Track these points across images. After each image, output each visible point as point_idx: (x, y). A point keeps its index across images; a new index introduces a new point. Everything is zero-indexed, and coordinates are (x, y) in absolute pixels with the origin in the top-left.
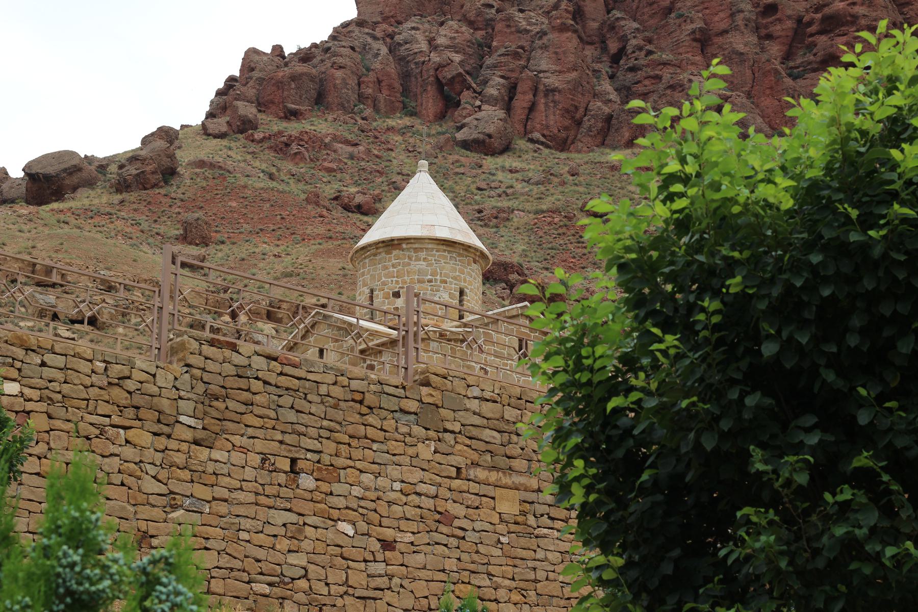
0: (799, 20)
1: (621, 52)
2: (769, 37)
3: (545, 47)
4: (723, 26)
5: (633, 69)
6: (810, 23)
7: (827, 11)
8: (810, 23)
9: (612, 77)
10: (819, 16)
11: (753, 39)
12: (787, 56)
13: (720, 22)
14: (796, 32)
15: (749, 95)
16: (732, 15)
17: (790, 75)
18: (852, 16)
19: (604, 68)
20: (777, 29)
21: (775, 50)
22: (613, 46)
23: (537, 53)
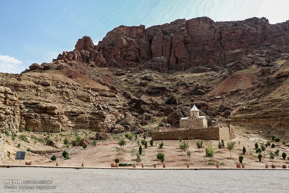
0: (125, 55)
11: (120, 56)
12: (123, 59)
13: (117, 54)
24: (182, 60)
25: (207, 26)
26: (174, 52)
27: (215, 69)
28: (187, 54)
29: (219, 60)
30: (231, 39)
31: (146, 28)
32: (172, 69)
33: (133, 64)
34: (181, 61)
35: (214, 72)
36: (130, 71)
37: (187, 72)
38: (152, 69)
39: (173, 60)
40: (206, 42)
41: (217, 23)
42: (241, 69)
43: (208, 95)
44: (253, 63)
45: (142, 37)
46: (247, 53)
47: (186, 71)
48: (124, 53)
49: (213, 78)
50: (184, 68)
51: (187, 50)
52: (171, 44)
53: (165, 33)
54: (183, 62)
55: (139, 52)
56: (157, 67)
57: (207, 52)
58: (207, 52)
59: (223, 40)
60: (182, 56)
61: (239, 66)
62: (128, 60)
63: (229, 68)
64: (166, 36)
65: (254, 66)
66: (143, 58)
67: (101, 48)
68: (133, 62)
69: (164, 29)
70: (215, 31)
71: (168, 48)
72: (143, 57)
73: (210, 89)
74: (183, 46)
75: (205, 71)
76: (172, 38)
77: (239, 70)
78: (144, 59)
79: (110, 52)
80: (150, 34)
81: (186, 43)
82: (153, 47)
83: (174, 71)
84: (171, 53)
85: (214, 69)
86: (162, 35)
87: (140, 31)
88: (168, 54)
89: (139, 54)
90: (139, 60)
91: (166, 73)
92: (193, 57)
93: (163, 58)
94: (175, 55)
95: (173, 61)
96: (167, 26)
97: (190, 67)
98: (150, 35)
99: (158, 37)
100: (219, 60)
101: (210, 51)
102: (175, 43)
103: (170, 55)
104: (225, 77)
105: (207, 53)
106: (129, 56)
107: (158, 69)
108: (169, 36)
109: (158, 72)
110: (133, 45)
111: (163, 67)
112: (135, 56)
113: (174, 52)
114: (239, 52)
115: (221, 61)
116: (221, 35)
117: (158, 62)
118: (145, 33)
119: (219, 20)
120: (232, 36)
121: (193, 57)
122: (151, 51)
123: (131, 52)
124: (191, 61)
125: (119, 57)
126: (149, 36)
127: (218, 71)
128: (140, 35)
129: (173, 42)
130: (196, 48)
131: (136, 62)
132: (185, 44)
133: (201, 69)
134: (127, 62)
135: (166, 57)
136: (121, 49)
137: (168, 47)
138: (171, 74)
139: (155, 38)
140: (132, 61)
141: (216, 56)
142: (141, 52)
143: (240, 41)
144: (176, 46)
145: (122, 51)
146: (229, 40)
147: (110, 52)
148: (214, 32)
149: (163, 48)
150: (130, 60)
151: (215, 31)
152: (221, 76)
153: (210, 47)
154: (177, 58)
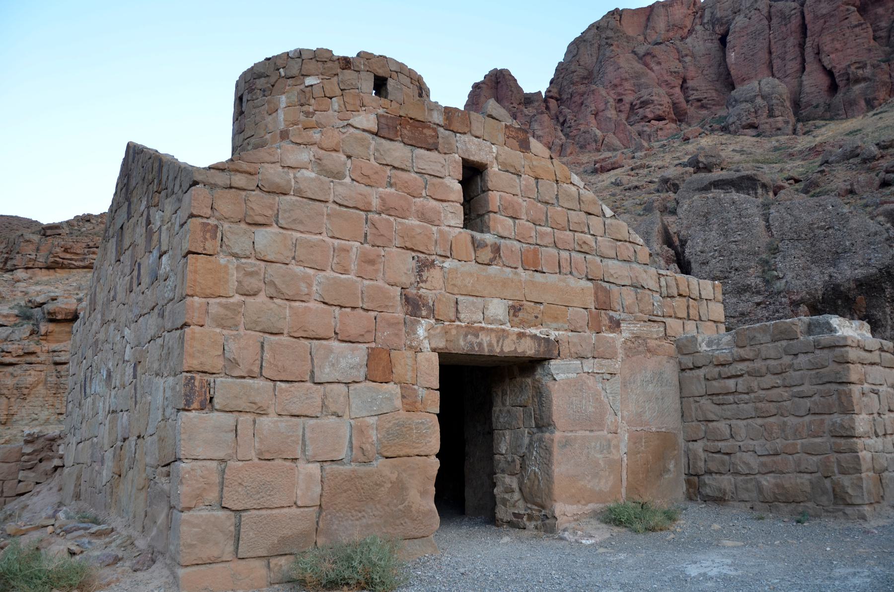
1: (565, 121)
2: (620, 111)
3: (536, 121)
4: (603, 108)
5: (569, 127)
6: (636, 105)
7: (641, 99)
8: (636, 105)
9: (562, 131)
10: (639, 102)
11: (614, 112)
12: (627, 118)
13: (601, 106)
14: (630, 109)
15: (614, 133)
16: (606, 104)
19: (559, 128)
20: (622, 108)
21: (623, 116)
22: (561, 120)
23: (533, 123)
24: (851, 76)
26: (818, 53)
28: (877, 44)
32: (814, 119)
33: (661, 129)
34: (848, 79)
37: (874, 115)
38: (730, 132)
45: (690, 32)
48: (629, 98)
50: (863, 103)
52: (804, 28)
54: (857, 81)
55: (682, 87)
56: (749, 121)
60: (854, 59)
62: (644, 118)
66: (702, 104)
67: (552, 97)
71: (789, 44)
72: (699, 100)
78: (703, 107)
79: (582, 104)
80: (718, 15)
82: (732, 56)
83: (823, 122)
84: (804, 61)
88: (793, 66)
89: (684, 93)
90: (686, 113)
93: (768, 83)
94: (820, 60)
95: (813, 89)
98: (717, 19)
99: (749, 16)
102: (816, 17)
103: (804, 69)
106: (644, 104)
107: (752, 126)
109: (754, 136)
110: (659, 63)
111: (771, 115)
112: (666, 100)
113: (818, 53)
117: (752, 100)
118: (701, 17)
122: (729, 74)
123: (650, 90)
125: (611, 113)
126: (714, 21)
129: (808, 18)
134: (638, 127)
135: (787, 79)
137: (792, 41)
140: (659, 119)
142: (690, 83)
144: (823, 29)
145: (619, 94)
147: (582, 104)
149: (770, 53)
150: (650, 116)
154: (830, 73)
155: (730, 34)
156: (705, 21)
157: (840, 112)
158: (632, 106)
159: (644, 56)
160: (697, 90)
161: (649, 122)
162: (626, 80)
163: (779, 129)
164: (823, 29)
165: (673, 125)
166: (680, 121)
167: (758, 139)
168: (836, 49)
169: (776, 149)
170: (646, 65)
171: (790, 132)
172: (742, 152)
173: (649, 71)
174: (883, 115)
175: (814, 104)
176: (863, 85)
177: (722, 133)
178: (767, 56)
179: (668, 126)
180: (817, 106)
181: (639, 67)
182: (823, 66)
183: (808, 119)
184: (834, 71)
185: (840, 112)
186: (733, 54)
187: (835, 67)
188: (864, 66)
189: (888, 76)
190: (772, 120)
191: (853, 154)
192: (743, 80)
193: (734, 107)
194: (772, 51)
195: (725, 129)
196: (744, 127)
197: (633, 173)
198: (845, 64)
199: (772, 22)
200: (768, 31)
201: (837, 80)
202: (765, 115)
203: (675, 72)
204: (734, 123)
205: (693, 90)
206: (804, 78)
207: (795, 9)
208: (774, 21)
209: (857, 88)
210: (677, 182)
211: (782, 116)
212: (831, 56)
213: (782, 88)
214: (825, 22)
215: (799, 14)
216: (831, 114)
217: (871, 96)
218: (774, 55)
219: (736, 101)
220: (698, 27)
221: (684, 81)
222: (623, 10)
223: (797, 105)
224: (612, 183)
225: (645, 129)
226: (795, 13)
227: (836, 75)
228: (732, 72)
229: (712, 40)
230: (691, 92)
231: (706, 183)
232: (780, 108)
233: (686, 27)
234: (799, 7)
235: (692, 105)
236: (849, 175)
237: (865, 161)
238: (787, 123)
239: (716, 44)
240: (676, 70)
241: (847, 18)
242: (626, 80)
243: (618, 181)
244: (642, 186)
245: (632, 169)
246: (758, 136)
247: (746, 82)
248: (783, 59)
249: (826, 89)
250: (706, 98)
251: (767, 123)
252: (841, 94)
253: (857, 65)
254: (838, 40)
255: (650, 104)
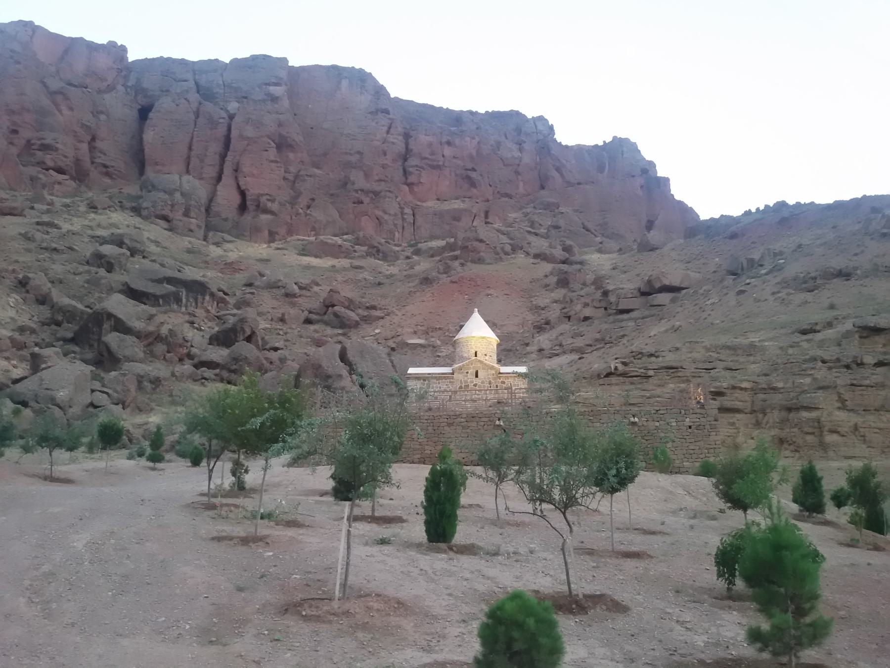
0: (28, 141)
2: (11, 143)
6: (33, 144)
10: (39, 142)
12: (18, 156)
17: (21, 164)
18: (56, 148)
21: (14, 150)
24: (261, 205)
25: (364, 101)
26: (236, 171)
27: (383, 253)
29: (395, 225)
30: (441, 163)
31: (132, 57)
32: (222, 232)
33: (59, 183)
35: (381, 262)
36: (45, 207)
38: (140, 215)
39: (227, 196)
40: (354, 159)
41: (397, 99)
42: (480, 261)
43: (377, 331)
44: (515, 249)
45: (111, 88)
46: (486, 217)
47: (273, 245)
48: (26, 134)
49: (381, 279)
50: (266, 233)
51: (285, 172)
53: (206, 94)
54: (266, 211)
55: (89, 143)
56: (163, 212)
57: (356, 191)
58: (356, 191)
59: (413, 161)
61: (475, 250)
62: (41, 164)
63: (432, 256)
64: (208, 107)
65: (520, 258)
68: (61, 177)
69: (203, 81)
70: (390, 128)
72: (105, 166)
73: (378, 313)
74: (272, 153)
75: (347, 254)
76: (231, 117)
77: (473, 262)
78: (108, 174)
81: (283, 145)
82: (149, 136)
85: (378, 251)
86: (194, 97)
87: (103, 62)
88: (210, 172)
89: (90, 151)
90: (88, 175)
91: (199, 240)
92: (303, 201)
93: (189, 182)
94: (236, 178)
96: (215, 71)
97: (290, 232)
100: (395, 225)
101: (366, 192)
102: (241, 137)
103: (219, 179)
104: (426, 281)
105: (357, 195)
106: (45, 148)
107: (166, 219)
108: (222, 109)
109: (165, 229)
110: (71, 109)
111: (186, 214)
114: (466, 210)
115: (401, 230)
116: (407, 144)
117: (170, 193)
119: (405, 96)
120: (443, 156)
121: (303, 201)
124: (298, 214)
126: (139, 90)
127: (391, 261)
128: (103, 80)
129: (234, 133)
130: (316, 170)
131: (73, 178)
132: (279, 147)
133: (333, 245)
134: (33, 171)
136: (12, 112)
137: (215, 148)
138: (217, 244)
139: (164, 104)
140: (60, 171)
141: (385, 212)
142: (98, 144)
143: (468, 178)
144: (245, 150)
146: (434, 167)
148: (385, 128)
149: (190, 149)
150: (50, 164)
151: (390, 128)
152: (408, 277)
153: (367, 176)
154: (243, 194)
155: (153, 110)
156: (130, 84)
157: (246, 234)
158: (29, 144)
159: (55, 93)
160: (105, 154)
161: (47, 170)
162: (28, 111)
163: (191, 231)
164: (245, 150)
165: (73, 183)
166: (80, 181)
167: (170, 233)
168: (253, 175)
169: (189, 251)
170: (56, 105)
171: (202, 238)
172: (157, 243)
173: (56, 112)
174: (285, 252)
175: (224, 216)
176: (269, 217)
177: (132, 214)
178: (186, 150)
179: (68, 182)
180: (226, 220)
181: (46, 102)
182: (238, 184)
183: (217, 230)
184: (247, 193)
185: (246, 234)
186: (152, 133)
187: (248, 190)
188: (273, 201)
189: (289, 217)
190: (186, 219)
191: (273, 286)
192: (157, 164)
193: (150, 192)
194: (193, 148)
195: (137, 211)
196: (158, 217)
197: (39, 227)
198: (256, 192)
199: (199, 119)
200: (193, 126)
201: (248, 203)
202: (181, 212)
203: (87, 126)
204: (147, 208)
205: (101, 152)
206: (219, 188)
207: (223, 118)
208: (201, 120)
209: (264, 217)
210: (113, 261)
211: (196, 219)
212: (248, 178)
213: (199, 189)
214: (248, 145)
215: (226, 125)
216: (239, 232)
217: (274, 230)
218: (193, 153)
219: (153, 186)
220: (120, 88)
221: (93, 139)
222: (38, 27)
223: (208, 210)
224: (20, 234)
225: (41, 176)
226: (223, 123)
227: (248, 198)
228: (147, 151)
229: (131, 107)
230: (99, 155)
231: (161, 276)
232: (196, 210)
233: (106, 80)
234: (227, 118)
235: (96, 168)
236: (275, 303)
237: (287, 295)
238: (199, 227)
239: (135, 114)
240: (89, 124)
241: (267, 151)
242: (28, 111)
243: (30, 235)
244: (63, 250)
245: (38, 223)
246: (170, 230)
247: (158, 167)
248: (202, 161)
249: (236, 206)
250: (113, 167)
251: (181, 221)
252: (249, 218)
253: (268, 197)
254: (256, 167)
255: (52, 150)
